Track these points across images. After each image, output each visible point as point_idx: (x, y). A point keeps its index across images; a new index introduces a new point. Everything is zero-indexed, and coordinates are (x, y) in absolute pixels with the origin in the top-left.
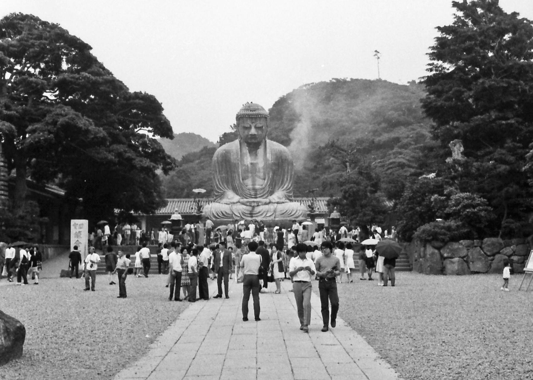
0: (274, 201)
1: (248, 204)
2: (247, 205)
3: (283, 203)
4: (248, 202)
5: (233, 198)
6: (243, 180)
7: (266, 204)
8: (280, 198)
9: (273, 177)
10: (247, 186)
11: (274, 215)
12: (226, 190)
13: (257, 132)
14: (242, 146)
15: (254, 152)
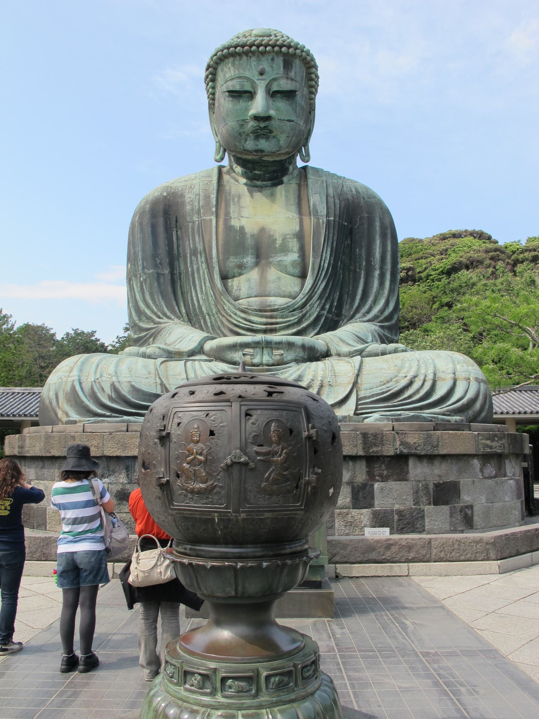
0: (345, 349)
1: (237, 356)
2: (234, 363)
3: (383, 353)
4: (234, 347)
5: (181, 339)
6: (224, 278)
7: (314, 355)
8: (364, 341)
9: (335, 267)
10: (237, 299)
11: (351, 404)
12: (166, 320)
13: (277, 110)
14: (226, 177)
15: (268, 191)
